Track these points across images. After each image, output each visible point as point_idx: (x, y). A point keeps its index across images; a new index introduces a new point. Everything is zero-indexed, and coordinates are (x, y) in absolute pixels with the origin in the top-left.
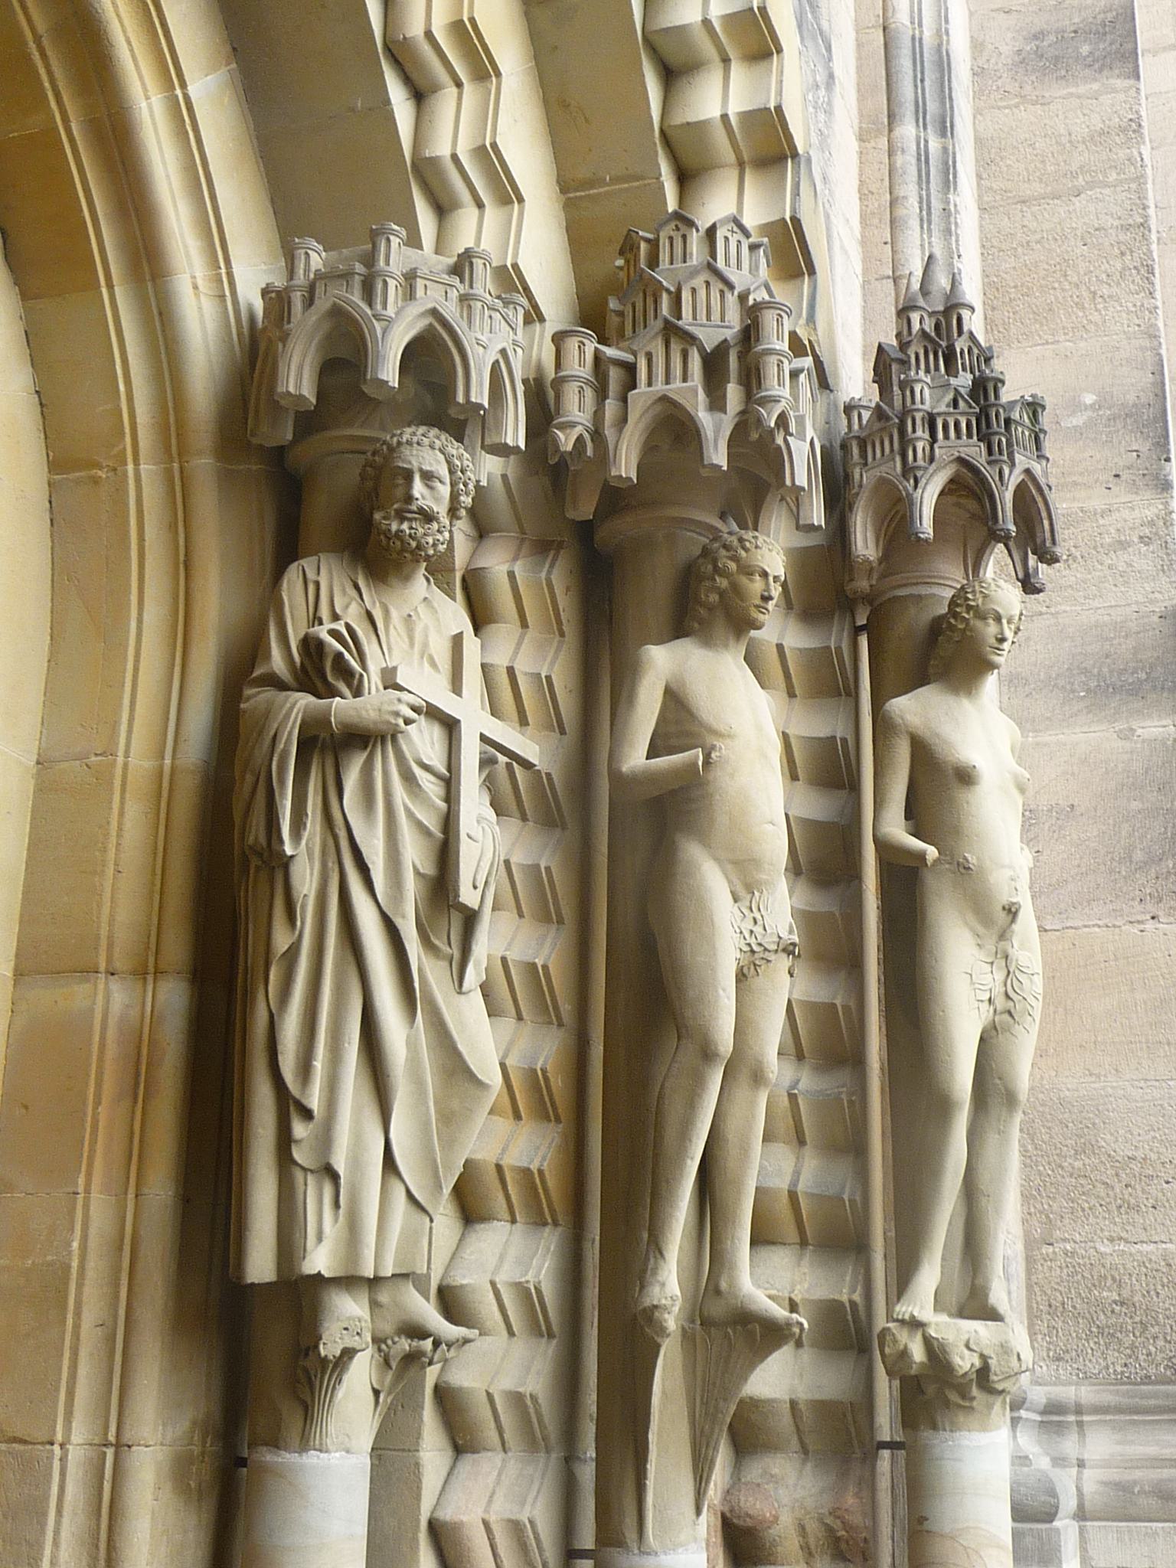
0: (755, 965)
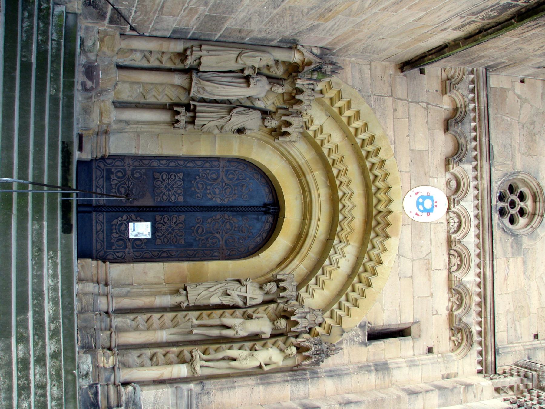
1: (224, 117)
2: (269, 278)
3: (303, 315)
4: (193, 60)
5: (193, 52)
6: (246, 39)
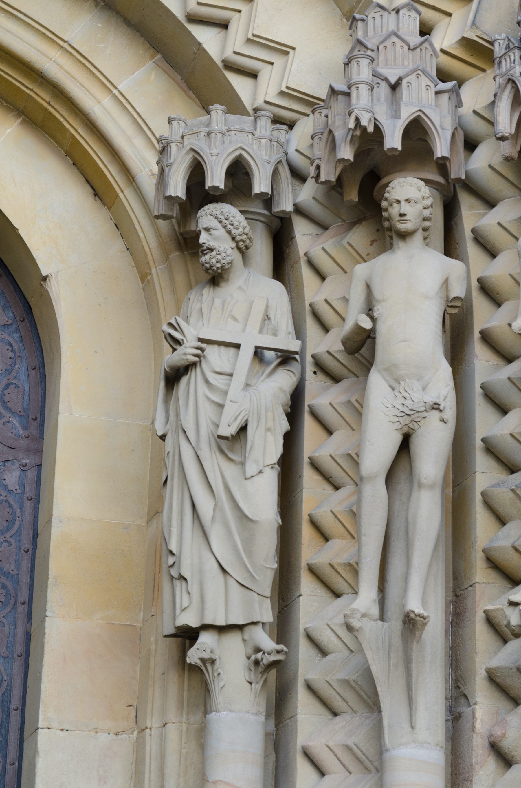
0: (416, 422)
2: (162, 244)
3: (384, 89)
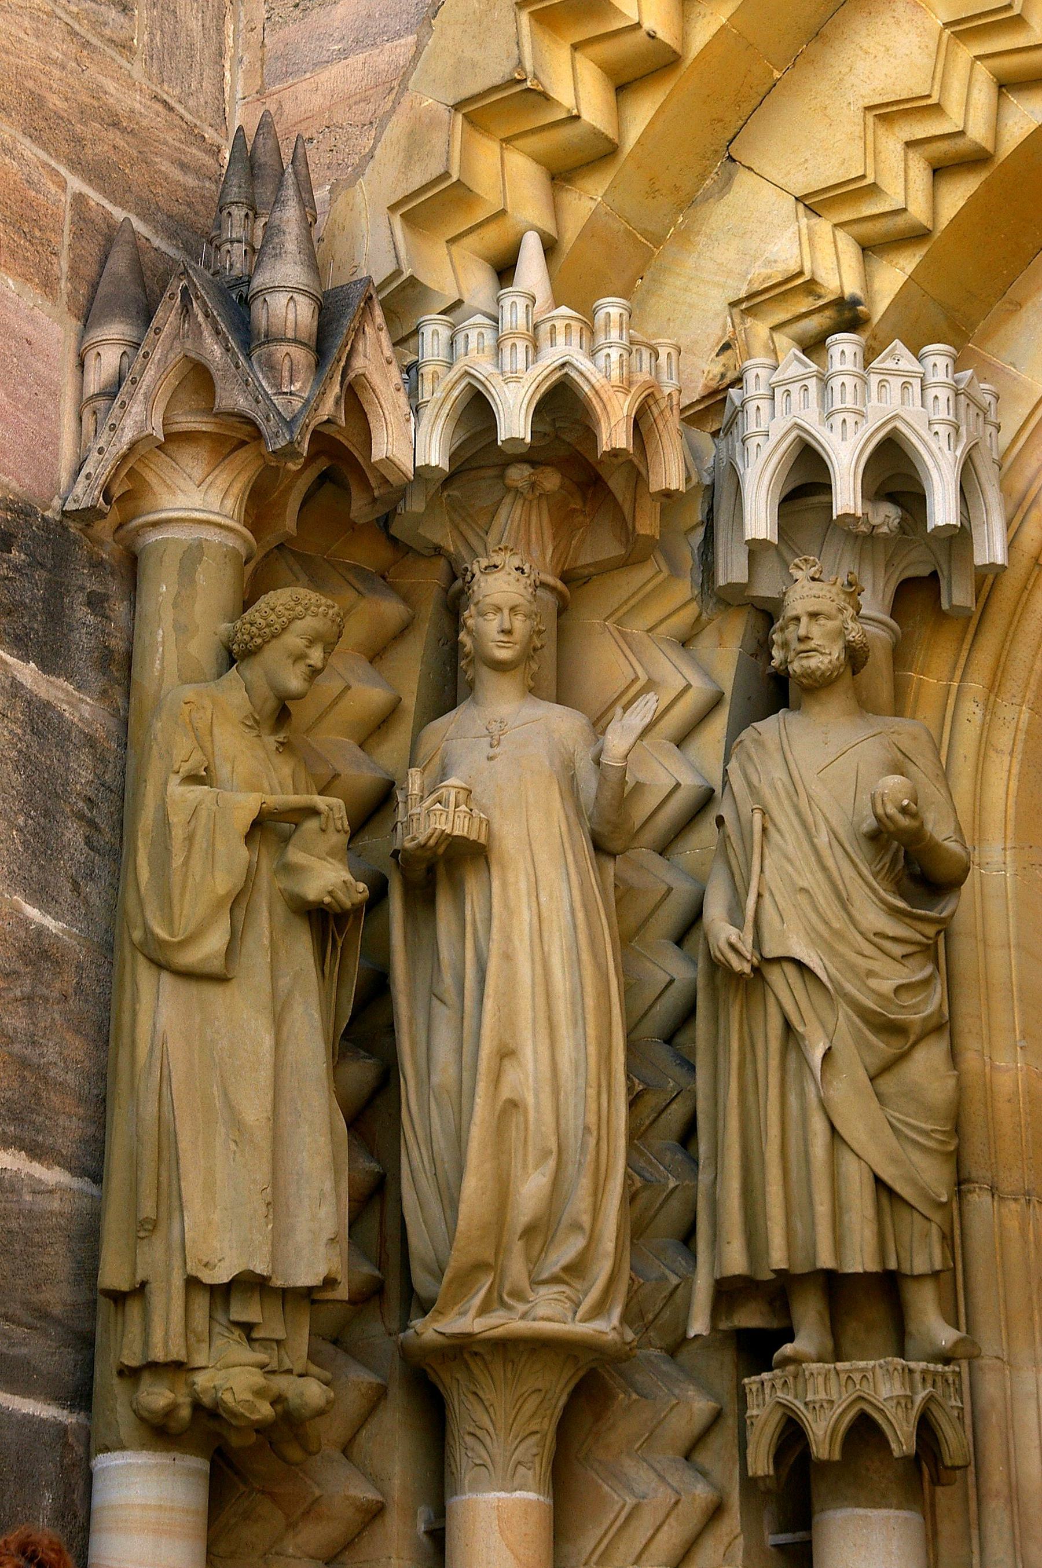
1: (788, 1027)
4: (245, 1354)
5: (158, 1354)
6: (41, 932)
